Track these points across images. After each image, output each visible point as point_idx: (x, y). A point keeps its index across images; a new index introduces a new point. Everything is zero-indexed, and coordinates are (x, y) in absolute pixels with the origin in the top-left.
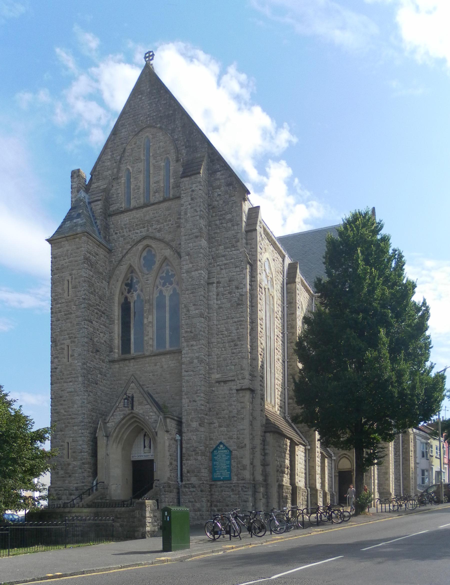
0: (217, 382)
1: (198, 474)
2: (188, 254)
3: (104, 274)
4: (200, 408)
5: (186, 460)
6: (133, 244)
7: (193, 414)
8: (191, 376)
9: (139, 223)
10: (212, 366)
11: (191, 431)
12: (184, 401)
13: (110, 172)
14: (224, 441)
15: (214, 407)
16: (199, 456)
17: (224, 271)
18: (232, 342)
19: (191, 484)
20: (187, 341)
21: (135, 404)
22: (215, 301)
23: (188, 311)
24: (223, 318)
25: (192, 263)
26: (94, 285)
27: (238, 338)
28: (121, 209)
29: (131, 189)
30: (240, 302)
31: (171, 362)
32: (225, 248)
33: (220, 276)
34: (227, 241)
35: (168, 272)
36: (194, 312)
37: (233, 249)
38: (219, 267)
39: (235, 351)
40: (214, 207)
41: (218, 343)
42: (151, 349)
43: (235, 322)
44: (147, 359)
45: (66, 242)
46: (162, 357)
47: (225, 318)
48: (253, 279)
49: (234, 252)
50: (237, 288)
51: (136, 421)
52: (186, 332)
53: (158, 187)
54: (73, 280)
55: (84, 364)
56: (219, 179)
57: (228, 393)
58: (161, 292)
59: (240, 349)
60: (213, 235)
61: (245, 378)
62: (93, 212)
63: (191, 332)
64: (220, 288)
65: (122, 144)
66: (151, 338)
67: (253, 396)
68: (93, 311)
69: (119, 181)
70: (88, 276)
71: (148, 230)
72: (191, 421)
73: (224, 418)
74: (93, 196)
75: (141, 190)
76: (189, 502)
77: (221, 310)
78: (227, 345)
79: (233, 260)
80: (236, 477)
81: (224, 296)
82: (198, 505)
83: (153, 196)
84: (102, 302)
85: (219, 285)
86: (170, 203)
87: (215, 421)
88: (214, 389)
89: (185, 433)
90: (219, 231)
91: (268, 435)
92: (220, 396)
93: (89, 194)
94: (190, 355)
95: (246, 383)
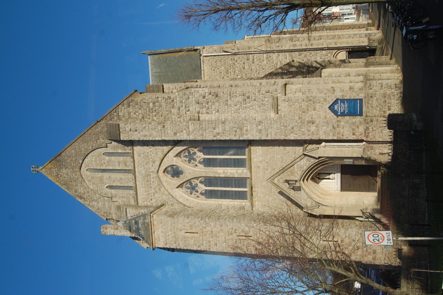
0: (278, 113)
2: (175, 134)
4: (298, 123)
6: (161, 185)
10: (264, 117)
15: (298, 115)
17: (191, 109)
18: (246, 100)
20: (242, 135)
23: (218, 134)
24: (227, 108)
25: (182, 132)
27: (243, 95)
28: (134, 194)
31: (257, 153)
32: (173, 107)
33: (194, 111)
34: (169, 106)
36: (220, 129)
37: (175, 101)
43: (231, 98)
44: (253, 175)
46: (252, 162)
47: (227, 106)
48: (199, 86)
49: (178, 99)
50: (204, 97)
52: (235, 135)
53: (122, 162)
55: (255, 221)
56: (124, 114)
57: (287, 103)
59: (253, 94)
60: (163, 117)
61: (276, 89)
62: (134, 215)
63: (236, 132)
64: (203, 111)
65: (88, 192)
69: (114, 195)
71: (153, 172)
72: (309, 132)
73: (308, 106)
75: (123, 177)
77: (220, 110)
78: (248, 105)
79: (183, 101)
81: (209, 108)
85: (200, 112)
86: (135, 152)
88: (283, 115)
89: (319, 137)
90: (161, 113)
92: (290, 109)
94: (254, 133)
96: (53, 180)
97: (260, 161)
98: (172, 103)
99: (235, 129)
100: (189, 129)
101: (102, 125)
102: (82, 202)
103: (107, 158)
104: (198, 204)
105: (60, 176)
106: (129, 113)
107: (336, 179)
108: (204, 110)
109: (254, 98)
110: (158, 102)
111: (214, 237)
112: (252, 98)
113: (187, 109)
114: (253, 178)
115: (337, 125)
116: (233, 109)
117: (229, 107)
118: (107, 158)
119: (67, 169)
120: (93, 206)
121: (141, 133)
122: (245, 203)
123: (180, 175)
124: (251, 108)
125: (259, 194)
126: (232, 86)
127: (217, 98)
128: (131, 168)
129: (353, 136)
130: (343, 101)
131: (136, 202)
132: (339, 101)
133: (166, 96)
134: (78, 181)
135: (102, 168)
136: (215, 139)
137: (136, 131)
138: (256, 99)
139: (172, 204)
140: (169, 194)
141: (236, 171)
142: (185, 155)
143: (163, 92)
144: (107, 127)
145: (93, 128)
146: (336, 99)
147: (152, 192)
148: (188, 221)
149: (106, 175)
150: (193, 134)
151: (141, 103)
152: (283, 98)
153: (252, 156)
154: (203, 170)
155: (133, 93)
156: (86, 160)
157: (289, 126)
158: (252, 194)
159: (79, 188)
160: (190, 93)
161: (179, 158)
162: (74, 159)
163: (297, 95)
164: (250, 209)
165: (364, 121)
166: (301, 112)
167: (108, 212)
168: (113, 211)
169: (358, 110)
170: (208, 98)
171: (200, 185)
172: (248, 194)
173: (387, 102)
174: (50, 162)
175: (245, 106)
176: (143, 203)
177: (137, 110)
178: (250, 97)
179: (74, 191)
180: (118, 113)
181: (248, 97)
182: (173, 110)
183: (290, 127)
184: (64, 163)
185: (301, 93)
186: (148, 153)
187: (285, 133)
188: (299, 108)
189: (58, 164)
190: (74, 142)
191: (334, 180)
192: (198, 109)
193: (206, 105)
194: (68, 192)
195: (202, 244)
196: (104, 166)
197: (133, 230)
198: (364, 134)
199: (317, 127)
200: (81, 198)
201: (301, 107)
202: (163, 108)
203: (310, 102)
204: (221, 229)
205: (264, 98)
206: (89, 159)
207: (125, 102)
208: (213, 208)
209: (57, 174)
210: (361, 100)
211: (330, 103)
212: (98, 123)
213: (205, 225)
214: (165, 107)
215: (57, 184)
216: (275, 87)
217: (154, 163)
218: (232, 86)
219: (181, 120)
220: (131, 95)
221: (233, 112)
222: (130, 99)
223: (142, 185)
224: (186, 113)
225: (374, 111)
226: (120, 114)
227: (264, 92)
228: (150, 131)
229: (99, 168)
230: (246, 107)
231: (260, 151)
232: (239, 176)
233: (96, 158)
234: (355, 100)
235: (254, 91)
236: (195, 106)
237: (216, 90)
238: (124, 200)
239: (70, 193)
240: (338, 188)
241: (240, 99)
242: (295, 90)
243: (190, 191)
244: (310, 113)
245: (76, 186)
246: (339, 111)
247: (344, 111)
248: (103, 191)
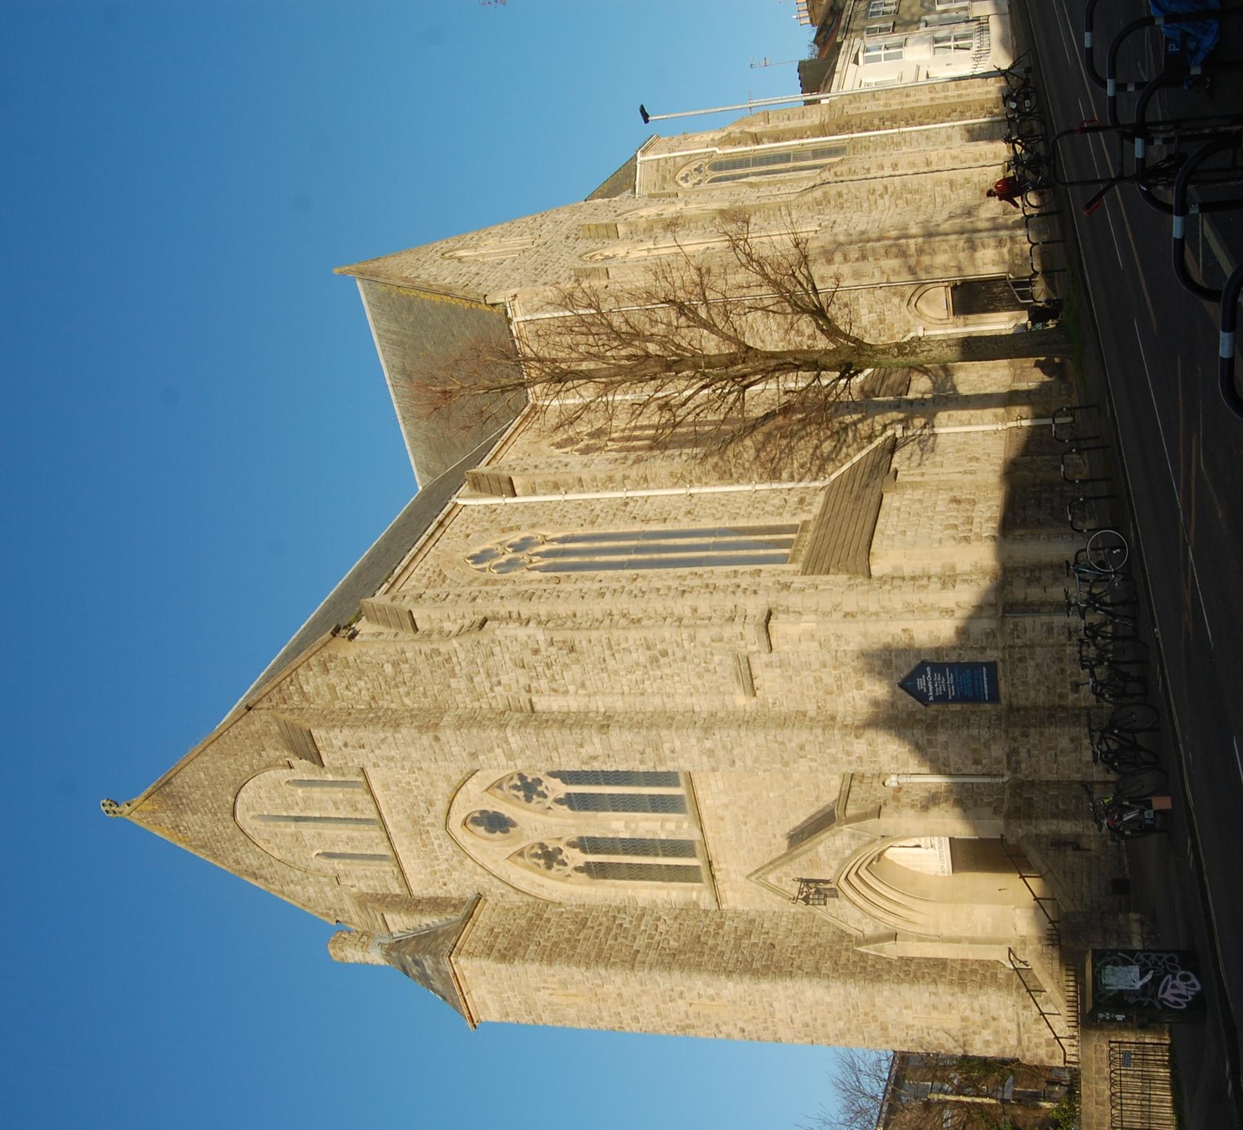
0: (755, 695)
1: (982, 741)
2: (474, 755)
3: (529, 914)
4: (816, 737)
7: (833, 751)
9: (419, 841)
11: (874, 753)
13: (327, 889)
16: (936, 740)
17: (504, 679)
18: (657, 661)
19: (1008, 756)
20: (661, 761)
23: (595, 758)
24: (606, 680)
25: (491, 750)
26: (556, 942)
27: (649, 648)
28: (395, 872)
29: (355, 852)
32: (453, 675)
33: (514, 685)
34: (439, 671)
35: (515, 787)
36: (598, 746)
37: (454, 659)
38: (495, 688)
40: (373, 698)
42: (685, 825)
43: (613, 655)
44: (709, 834)
45: (473, 993)
46: (702, 807)
47: (606, 675)
48: (515, 615)
49: (462, 656)
52: (642, 762)
54: (548, 985)
57: (778, 670)
58: (559, 801)
63: (642, 753)
65: (271, 865)
66: (662, 826)
67: (783, 612)
68: (611, 947)
69: (341, 873)
70: (540, 958)
71: (433, 825)
75: (356, 834)
77: (588, 683)
78: (667, 671)
79: (479, 661)
80: (988, 652)
81: (557, 678)
82: (1064, 743)
83: (364, 813)
84: (589, 924)
85: (533, 690)
86: (373, 782)
88: (770, 701)
90: (422, 689)
91: (876, 570)
95: (752, 632)
96: (167, 838)
97: (723, 805)
98: (447, 665)
99: (640, 748)
100: (509, 744)
101: (265, 718)
102: (263, 887)
103: (300, 791)
104: (572, 895)
105: (185, 829)
106: (332, 688)
107: (937, 846)
108: (543, 683)
109: (679, 654)
110: (406, 661)
111: (629, 1005)
112: (674, 654)
113: (494, 679)
114: (710, 842)
115: (928, 740)
116: (624, 681)
117: (612, 677)
118: (300, 791)
119: (199, 814)
120: (293, 895)
121: (377, 752)
122: (698, 894)
123: (511, 829)
124: (676, 678)
125: (733, 876)
126: (610, 614)
127: (574, 654)
128: (371, 814)
129: (974, 767)
130: (939, 668)
131: (405, 889)
132: (928, 668)
133: (426, 648)
134: (237, 840)
135: (293, 814)
136: (586, 768)
138: (688, 657)
139: (502, 895)
140: (490, 873)
141: (659, 824)
142: (512, 783)
143: (416, 629)
144: (279, 726)
145: (239, 723)
146: (919, 662)
147: (444, 866)
148: (552, 972)
149: (308, 830)
150: (523, 756)
151: (360, 665)
152: (763, 661)
153: (699, 793)
154: (570, 822)
155: (330, 640)
156: (242, 794)
157: (790, 740)
158: (713, 876)
159: (244, 856)
160: (493, 641)
161: (499, 791)
162: (210, 792)
163: (803, 646)
164: (714, 907)
165: (1004, 735)
166: (820, 693)
167: (336, 907)
168: (349, 905)
169: (986, 691)
170: (548, 653)
172: (704, 873)
173: (1069, 672)
174: (147, 798)
175: (659, 673)
176: (425, 892)
177: (352, 680)
178: (670, 653)
179: (231, 861)
180: (301, 687)
181: (665, 654)
182: (453, 683)
183: (794, 744)
184: (184, 801)
185: (816, 644)
186: (409, 783)
187: (782, 758)
188: (816, 682)
189: (170, 802)
190: (199, 754)
191: (931, 850)
192: (524, 681)
193: (547, 672)
194: (218, 864)
195: (601, 1019)
196: (297, 809)
197: (414, 975)
198: (1005, 761)
199: (870, 745)
200: (255, 876)
201: (818, 680)
202: (425, 677)
203: (843, 668)
204: (643, 991)
205: (709, 656)
206: (252, 794)
207: (313, 661)
208: (613, 904)
209: (174, 824)
210: (992, 667)
211: (902, 672)
212: (251, 712)
213: (599, 982)
214: (429, 675)
215: (183, 846)
216: (737, 629)
217: (431, 806)
219: (483, 705)
220: (325, 645)
221: (626, 689)
223: (411, 852)
224: (491, 689)
225: (1032, 694)
226: (306, 688)
227: (707, 641)
229: (285, 814)
230: (661, 678)
231: (720, 784)
233: (270, 793)
234: (975, 666)
235: (679, 639)
236: (514, 674)
237: (568, 635)
238: (372, 883)
239: (224, 867)
240: (946, 868)
241: (642, 656)
242: (796, 637)
243: (547, 847)
244: (849, 695)
245: (234, 851)
246: (931, 694)
247: (945, 694)
248: (311, 865)
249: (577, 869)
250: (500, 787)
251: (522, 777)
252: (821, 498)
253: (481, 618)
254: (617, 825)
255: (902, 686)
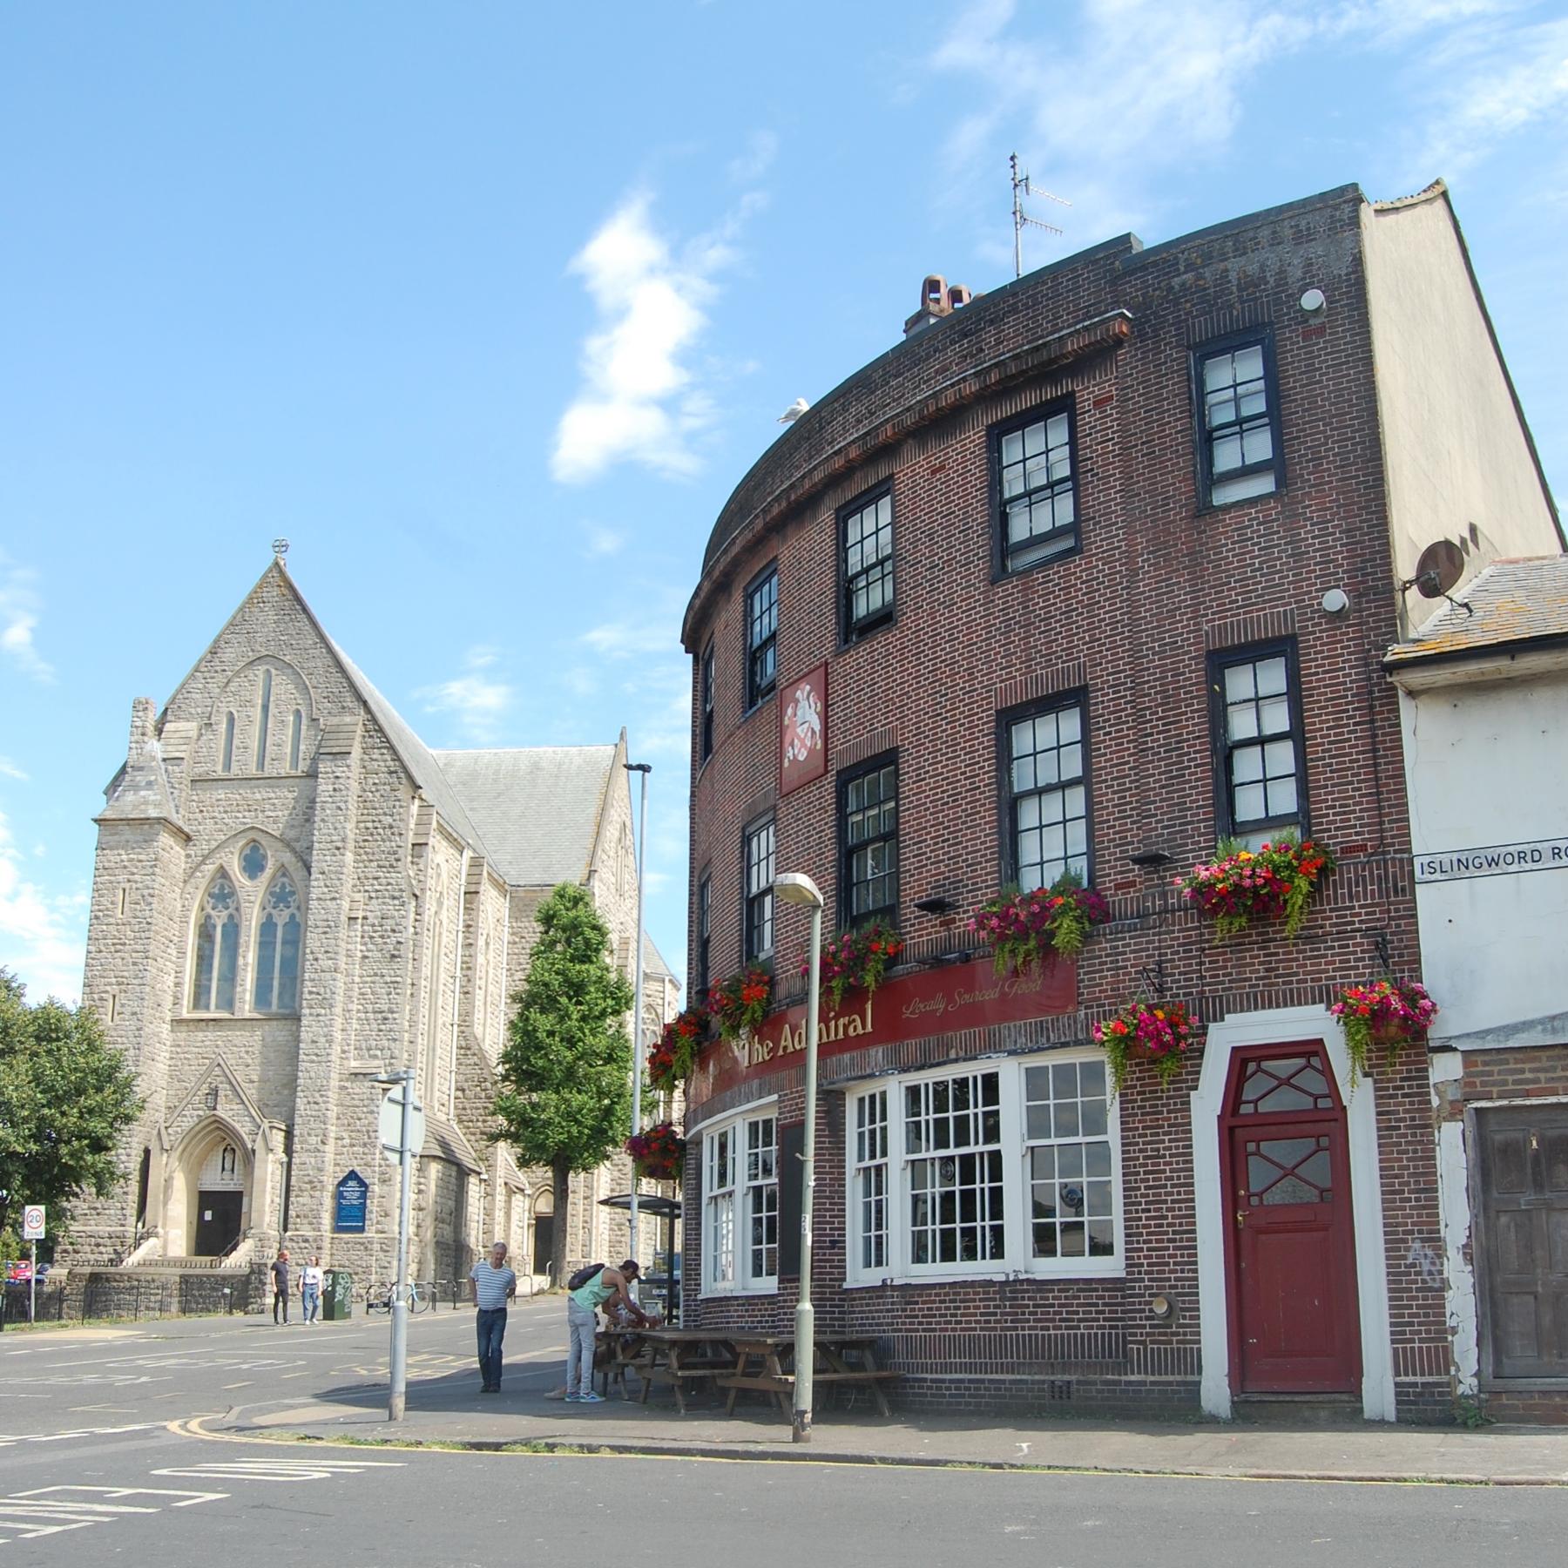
5: (297, 1196)
8: (313, 1062)
12: (298, 1100)
14: (357, 1169)
17: (374, 901)
21: (222, 1099)
22: (359, 947)
30: (396, 953)
39: (383, 1027)
41: (358, 1011)
50: (394, 931)
51: (218, 1128)
52: (311, 993)
58: (270, 916)
63: (318, 994)
74: (170, 748)
76: (298, 1264)
87: (345, 1135)
93: (162, 742)
94: (314, 1029)
130: (364, 1195)
135: (272, 706)
137: (335, 790)
171: (226, 913)
218: (413, 985)
222: (402, 775)
228: (332, 820)
232: (238, 996)
247: (345, 1198)
249: (208, 917)
250: (284, 875)
251: (293, 893)
252: (443, 1118)
253: (418, 893)
254: (249, 958)
255: (352, 1172)
